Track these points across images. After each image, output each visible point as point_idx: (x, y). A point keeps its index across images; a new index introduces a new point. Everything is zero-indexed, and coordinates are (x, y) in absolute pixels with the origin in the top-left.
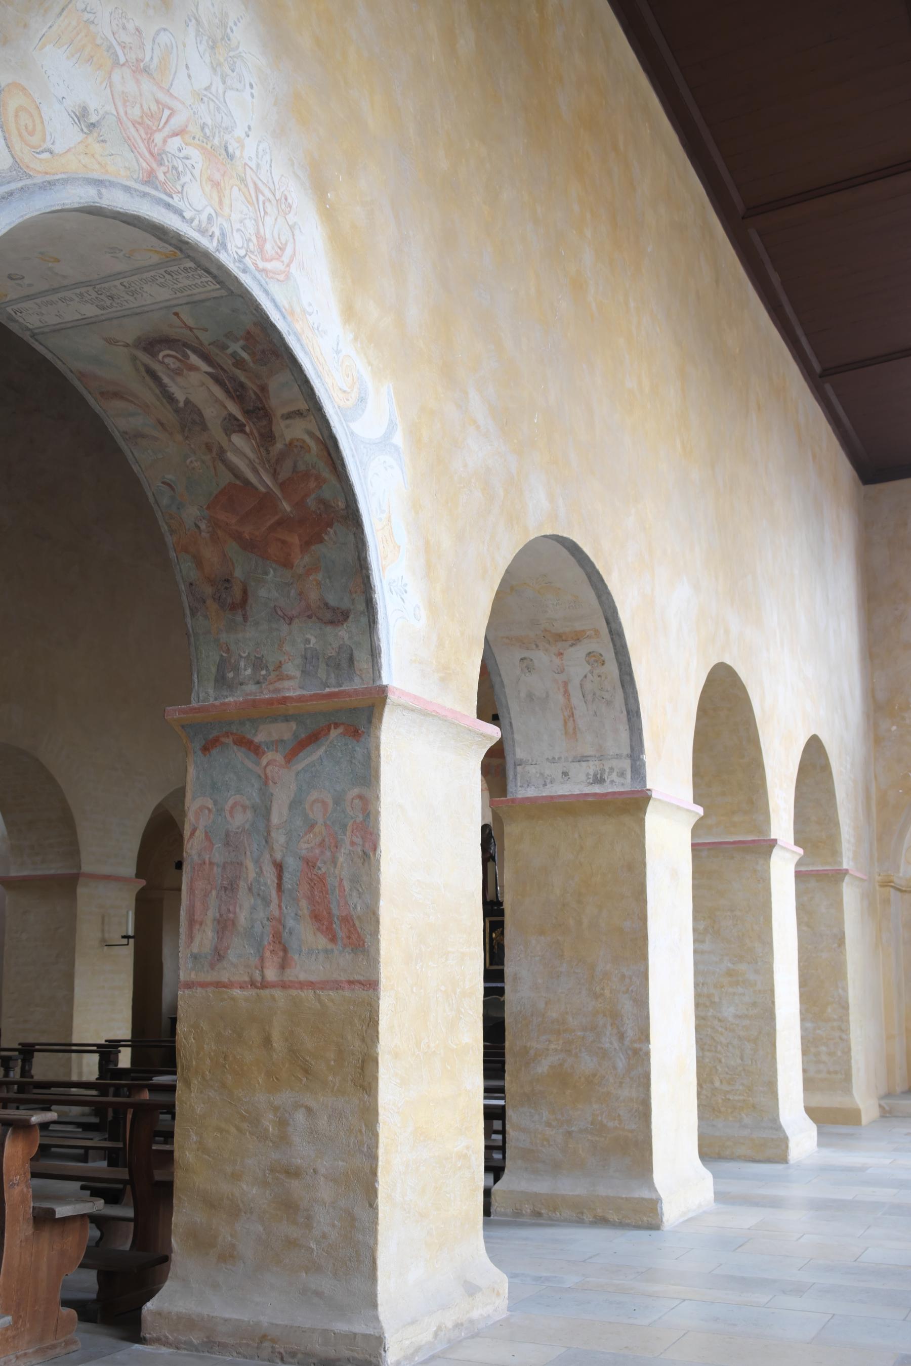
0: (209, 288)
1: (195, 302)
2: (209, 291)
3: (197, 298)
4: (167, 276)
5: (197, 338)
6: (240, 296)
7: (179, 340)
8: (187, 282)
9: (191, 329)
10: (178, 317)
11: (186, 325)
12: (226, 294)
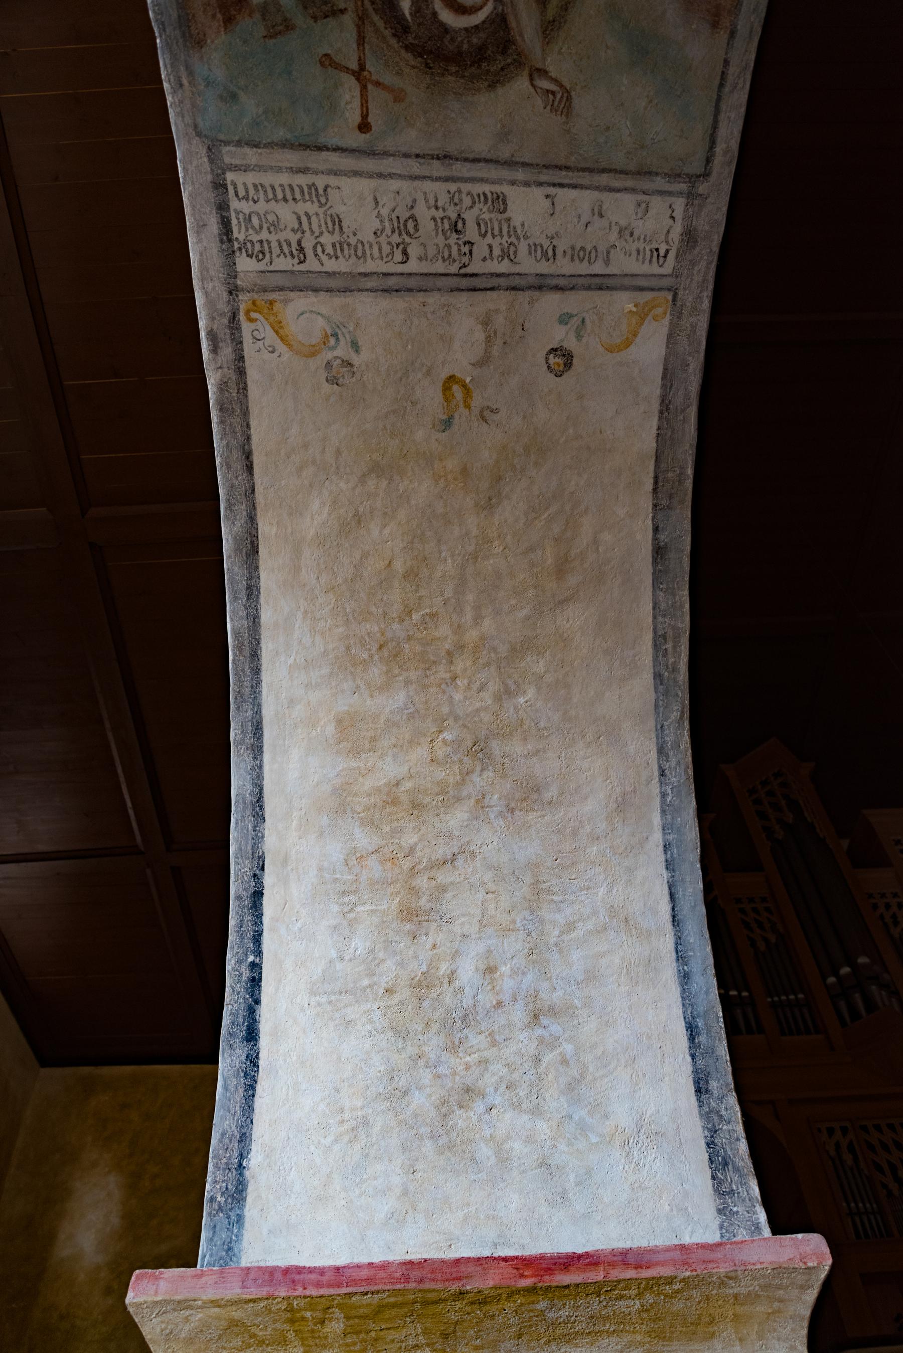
0: (251, 178)
1: (305, 147)
2: (259, 168)
3: (292, 158)
4: (308, 244)
5: (361, 40)
6: (199, 134)
7: (407, 48)
8: (285, 213)
9: (359, 74)
10: (365, 116)
11: (364, 88)
12: (225, 149)
